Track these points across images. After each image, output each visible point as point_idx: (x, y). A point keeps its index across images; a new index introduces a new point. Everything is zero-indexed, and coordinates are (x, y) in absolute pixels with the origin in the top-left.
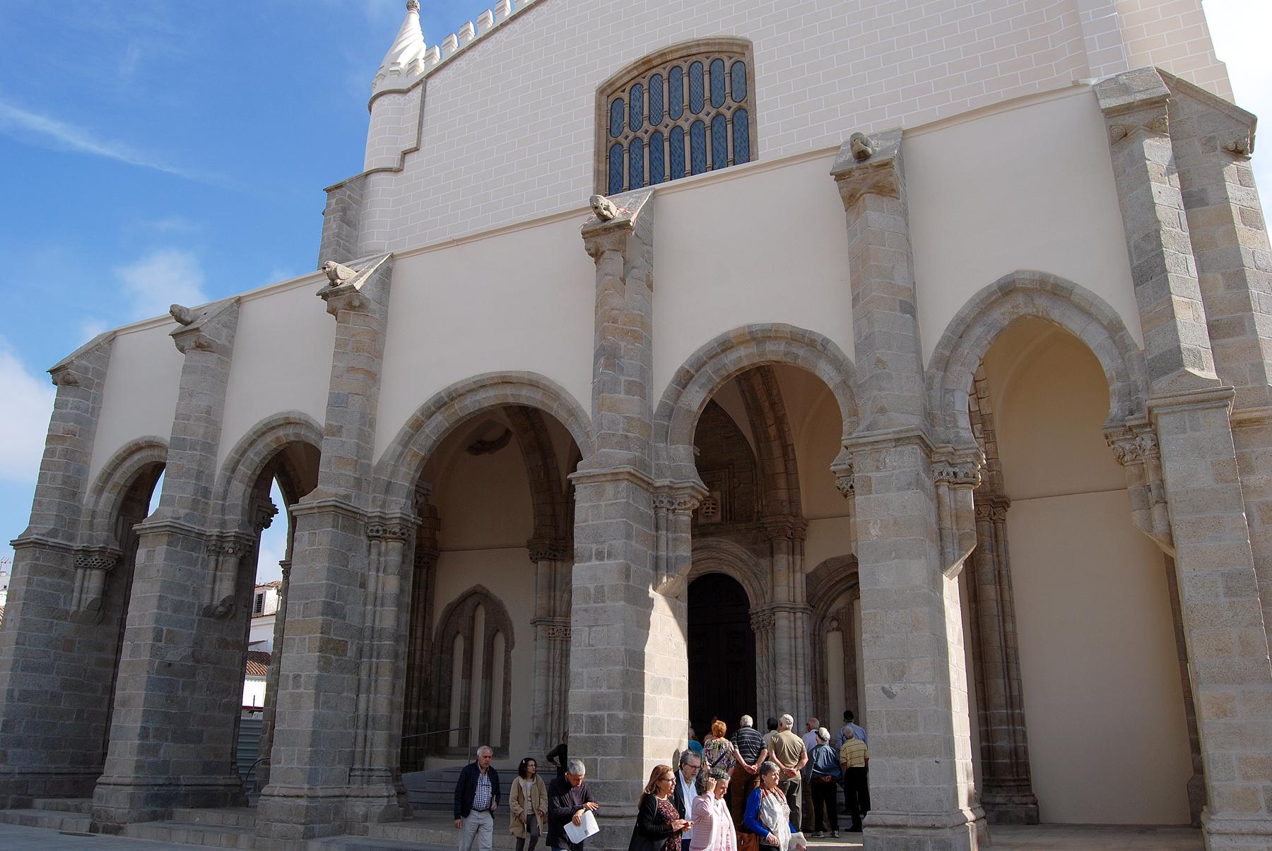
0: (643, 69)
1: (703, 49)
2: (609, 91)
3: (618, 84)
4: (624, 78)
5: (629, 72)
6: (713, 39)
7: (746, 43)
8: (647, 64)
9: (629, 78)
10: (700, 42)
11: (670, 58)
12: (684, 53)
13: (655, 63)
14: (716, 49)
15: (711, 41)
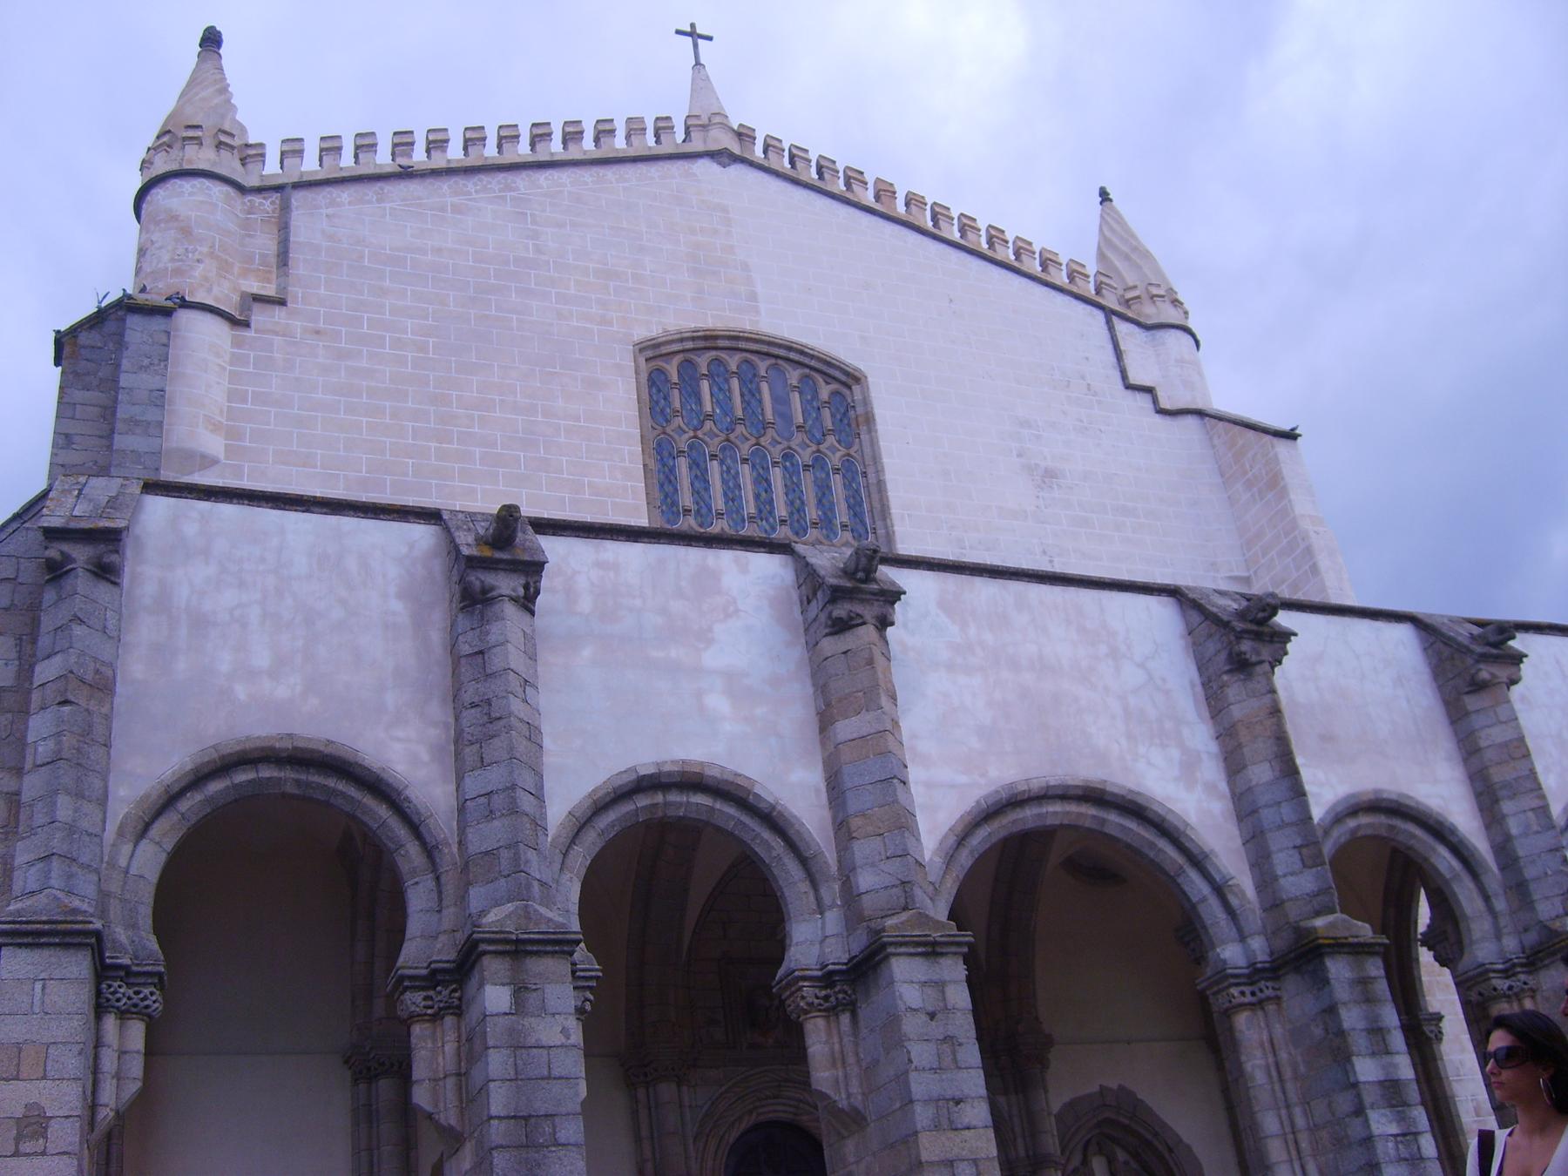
0: (701, 344)
1: (792, 355)
2: (650, 353)
3: (664, 350)
4: (673, 346)
5: (682, 340)
6: (811, 349)
7: (856, 374)
8: (708, 341)
9: (681, 348)
10: (795, 346)
11: (744, 346)
12: (765, 348)
13: (721, 343)
14: (813, 363)
15: (806, 350)
